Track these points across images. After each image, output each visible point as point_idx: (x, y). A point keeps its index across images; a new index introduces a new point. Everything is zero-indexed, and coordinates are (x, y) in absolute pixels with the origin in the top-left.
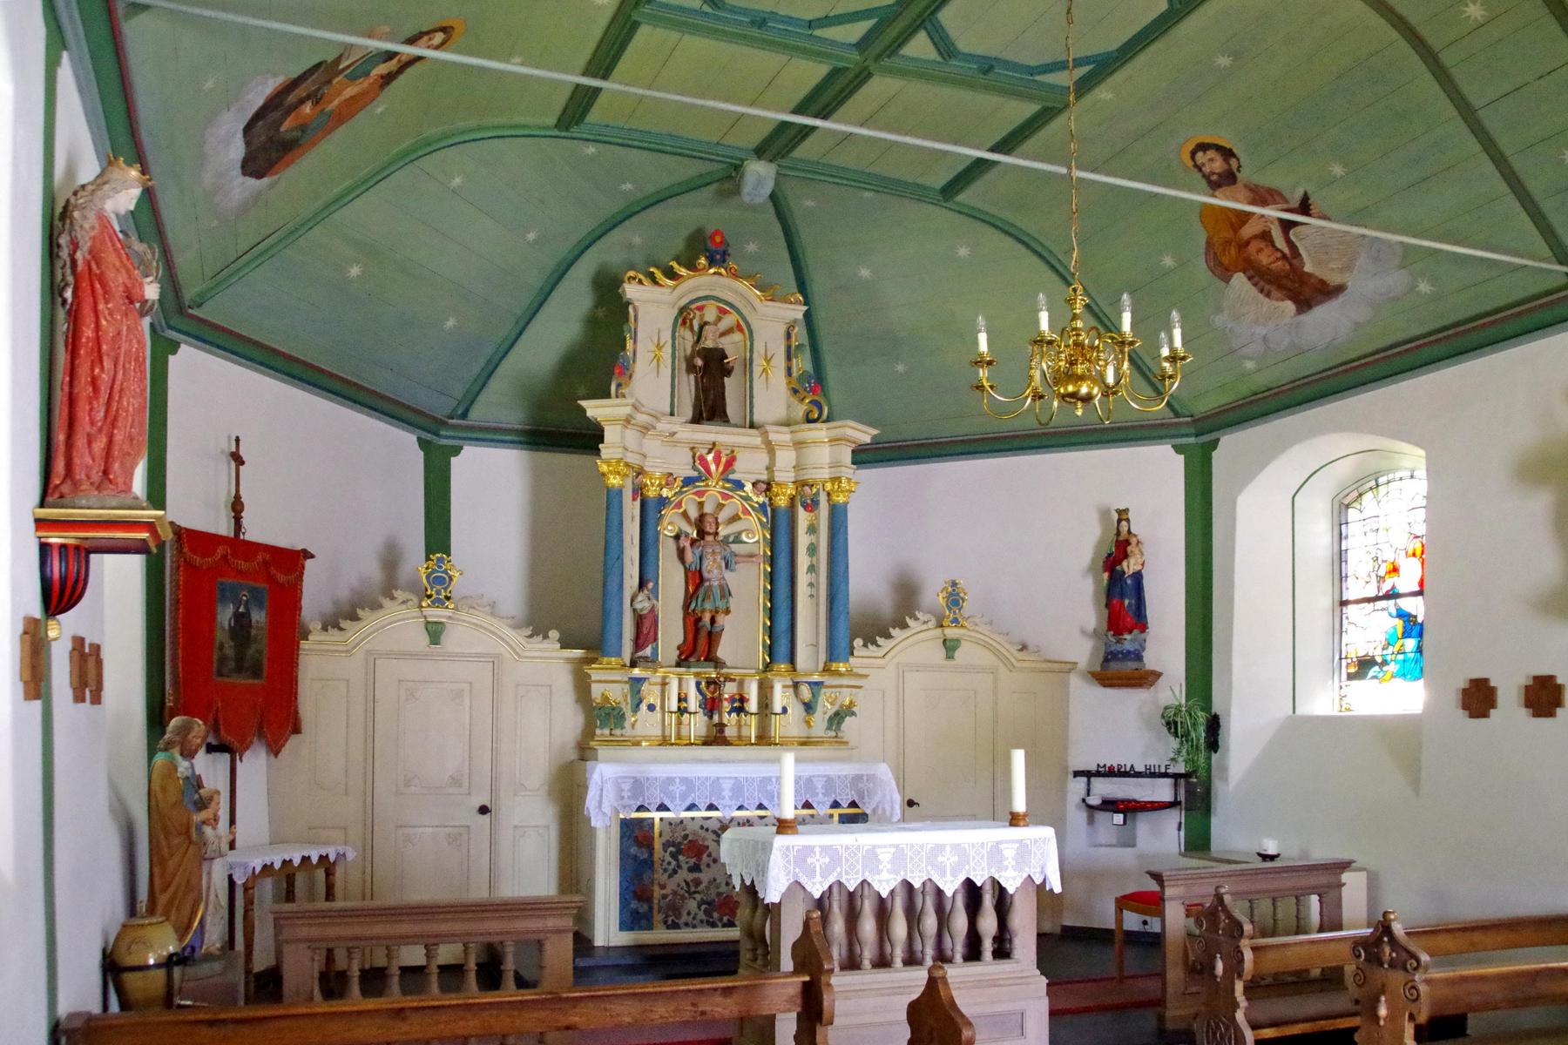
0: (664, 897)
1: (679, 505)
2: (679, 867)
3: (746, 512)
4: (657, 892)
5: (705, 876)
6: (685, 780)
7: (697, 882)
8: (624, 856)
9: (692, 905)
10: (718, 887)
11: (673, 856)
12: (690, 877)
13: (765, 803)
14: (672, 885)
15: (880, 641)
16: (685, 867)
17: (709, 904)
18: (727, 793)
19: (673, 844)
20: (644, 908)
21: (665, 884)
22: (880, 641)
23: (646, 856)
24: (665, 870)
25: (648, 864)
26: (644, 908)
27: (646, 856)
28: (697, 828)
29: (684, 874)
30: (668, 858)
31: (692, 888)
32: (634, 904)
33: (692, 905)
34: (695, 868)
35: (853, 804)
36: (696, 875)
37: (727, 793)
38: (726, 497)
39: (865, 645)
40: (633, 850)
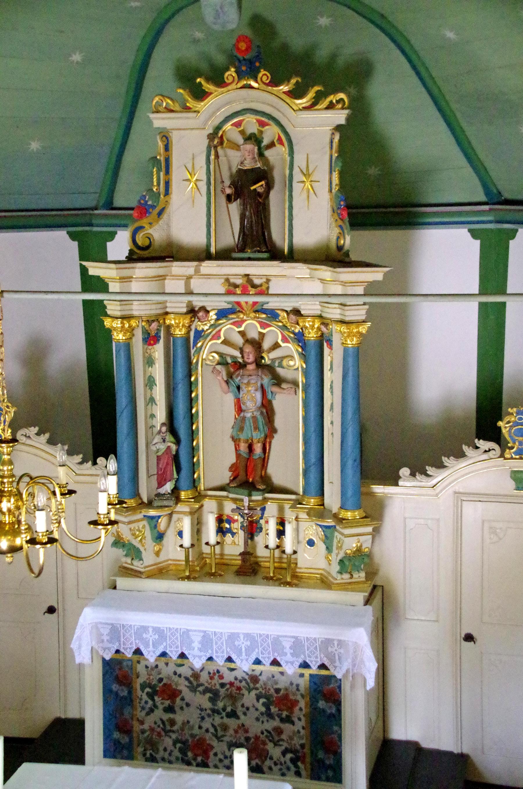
0: (143, 732)
1: (217, 336)
2: (155, 706)
3: (285, 339)
4: (137, 727)
5: (179, 718)
6: (158, 631)
7: (172, 722)
8: (107, 691)
9: (168, 742)
10: (192, 728)
11: (151, 696)
12: (166, 717)
13: (234, 657)
14: (149, 721)
15: (430, 470)
16: (161, 707)
17: (184, 743)
18: (196, 645)
19: (150, 686)
20: (125, 740)
21: (147, 719)
22: (430, 470)
23: (125, 693)
24: (143, 708)
25: (130, 700)
26: (125, 740)
27: (125, 693)
28: (172, 674)
29: (159, 713)
30: (145, 697)
31: (167, 727)
32: (116, 735)
33: (168, 742)
34: (170, 709)
35: (323, 666)
36: (171, 716)
37: (196, 645)
38: (264, 325)
39: (413, 474)
40: (115, 687)
